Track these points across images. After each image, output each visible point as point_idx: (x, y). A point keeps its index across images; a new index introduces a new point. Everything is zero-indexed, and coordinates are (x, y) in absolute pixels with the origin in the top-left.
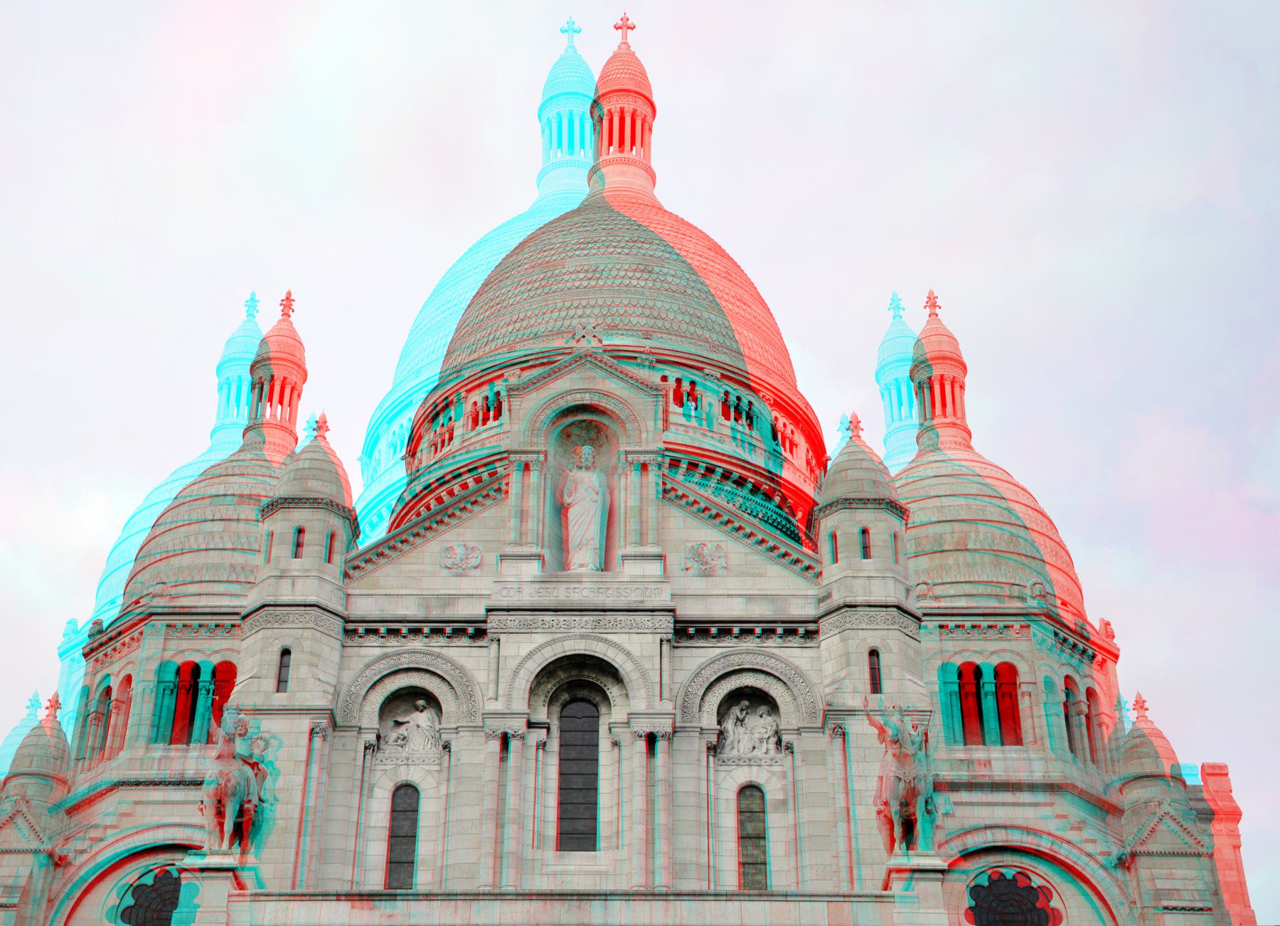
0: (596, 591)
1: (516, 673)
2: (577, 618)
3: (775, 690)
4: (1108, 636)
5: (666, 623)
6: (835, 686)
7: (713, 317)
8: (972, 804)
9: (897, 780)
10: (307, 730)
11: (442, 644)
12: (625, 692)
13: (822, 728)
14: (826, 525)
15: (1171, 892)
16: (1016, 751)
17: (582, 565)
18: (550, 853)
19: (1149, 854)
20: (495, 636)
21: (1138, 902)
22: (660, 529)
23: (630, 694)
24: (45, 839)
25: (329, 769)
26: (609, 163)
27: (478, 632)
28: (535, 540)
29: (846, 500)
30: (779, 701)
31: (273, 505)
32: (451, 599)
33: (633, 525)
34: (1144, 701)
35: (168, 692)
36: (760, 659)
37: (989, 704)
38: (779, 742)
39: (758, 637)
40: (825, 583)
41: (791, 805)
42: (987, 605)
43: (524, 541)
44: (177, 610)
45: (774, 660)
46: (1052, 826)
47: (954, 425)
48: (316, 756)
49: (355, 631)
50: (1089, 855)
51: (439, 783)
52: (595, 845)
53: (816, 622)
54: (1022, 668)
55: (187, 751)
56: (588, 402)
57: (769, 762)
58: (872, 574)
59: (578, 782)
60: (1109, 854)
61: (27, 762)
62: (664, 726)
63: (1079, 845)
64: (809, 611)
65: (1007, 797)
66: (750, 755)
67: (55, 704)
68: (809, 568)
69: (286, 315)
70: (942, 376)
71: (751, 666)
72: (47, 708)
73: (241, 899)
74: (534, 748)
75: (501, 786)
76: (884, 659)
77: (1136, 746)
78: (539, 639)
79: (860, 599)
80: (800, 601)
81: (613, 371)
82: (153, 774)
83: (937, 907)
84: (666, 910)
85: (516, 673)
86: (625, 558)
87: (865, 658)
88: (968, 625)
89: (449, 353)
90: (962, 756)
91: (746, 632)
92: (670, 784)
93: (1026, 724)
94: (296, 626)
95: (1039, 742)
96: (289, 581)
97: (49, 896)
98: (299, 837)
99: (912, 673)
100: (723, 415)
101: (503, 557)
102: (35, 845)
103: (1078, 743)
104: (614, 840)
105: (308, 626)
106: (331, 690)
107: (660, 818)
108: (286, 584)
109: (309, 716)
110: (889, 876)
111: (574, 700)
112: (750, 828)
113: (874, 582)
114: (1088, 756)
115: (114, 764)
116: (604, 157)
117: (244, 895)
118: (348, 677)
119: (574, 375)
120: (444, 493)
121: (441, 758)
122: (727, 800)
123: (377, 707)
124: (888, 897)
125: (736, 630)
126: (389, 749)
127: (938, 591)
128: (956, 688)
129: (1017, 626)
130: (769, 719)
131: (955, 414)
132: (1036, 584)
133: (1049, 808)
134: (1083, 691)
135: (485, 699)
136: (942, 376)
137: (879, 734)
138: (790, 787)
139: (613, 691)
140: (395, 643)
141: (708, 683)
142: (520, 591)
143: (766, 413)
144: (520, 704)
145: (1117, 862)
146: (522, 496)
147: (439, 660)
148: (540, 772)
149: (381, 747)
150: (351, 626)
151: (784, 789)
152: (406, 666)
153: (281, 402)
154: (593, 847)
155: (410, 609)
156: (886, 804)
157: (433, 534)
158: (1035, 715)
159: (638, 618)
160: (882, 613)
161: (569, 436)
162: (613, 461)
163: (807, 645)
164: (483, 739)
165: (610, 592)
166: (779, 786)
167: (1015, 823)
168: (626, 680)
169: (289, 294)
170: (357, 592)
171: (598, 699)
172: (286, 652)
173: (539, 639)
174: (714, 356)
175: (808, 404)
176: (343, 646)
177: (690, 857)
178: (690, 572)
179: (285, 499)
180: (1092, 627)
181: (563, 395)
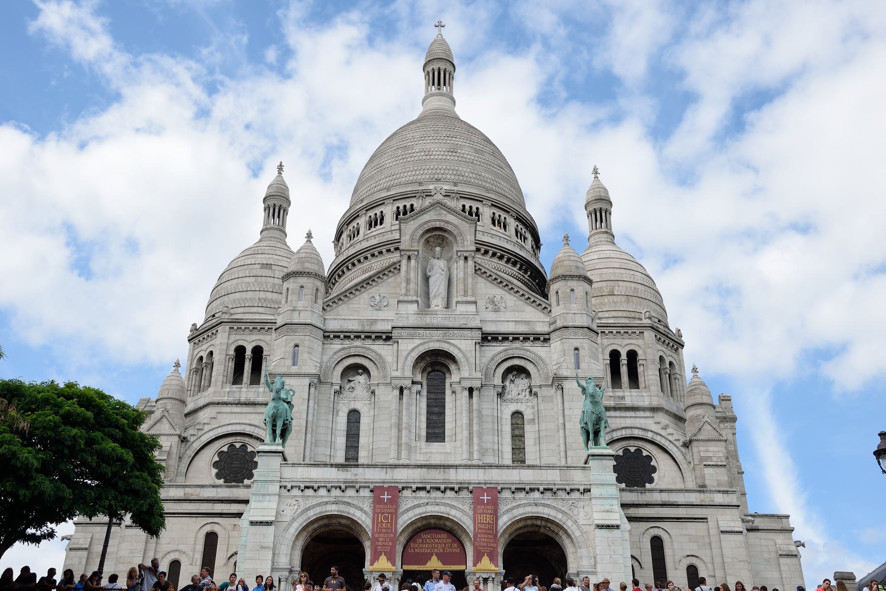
1: (406, 358)
2: (435, 332)
4: (679, 336)
5: (478, 335)
6: (558, 366)
7: (487, 175)
8: (616, 417)
10: (308, 385)
11: (370, 343)
12: (458, 367)
13: (552, 385)
14: (553, 288)
15: (709, 458)
16: (636, 392)
17: (436, 306)
18: (423, 443)
19: (698, 440)
21: (692, 463)
22: (474, 289)
23: (461, 369)
24: (177, 429)
25: (318, 402)
26: (433, 95)
31: (288, 275)
32: (374, 321)
33: (461, 286)
34: (697, 368)
35: (231, 360)
37: (624, 370)
38: (531, 391)
40: (553, 316)
41: (536, 421)
42: (623, 322)
43: (408, 293)
44: (234, 320)
47: (607, 232)
48: (312, 397)
49: (329, 336)
50: (670, 441)
51: (370, 410)
52: (444, 440)
53: (549, 334)
54: (640, 352)
55: (241, 388)
56: (439, 226)
57: (526, 401)
59: (436, 410)
60: (678, 440)
61: (166, 392)
62: (476, 384)
65: (632, 414)
66: (517, 398)
67: (177, 365)
69: (280, 173)
70: (601, 208)
71: (518, 355)
72: (174, 367)
73: (286, 465)
75: (400, 411)
76: (581, 352)
77: (693, 390)
78: (417, 342)
79: (570, 324)
80: (542, 324)
82: (226, 399)
84: (485, 473)
85: (406, 358)
86: (457, 302)
87: (572, 352)
88: (614, 332)
89: (356, 190)
90: (611, 394)
91: (515, 339)
92: (479, 412)
93: (641, 379)
94: (301, 334)
95: (647, 387)
96: (297, 312)
97: (179, 456)
98: (306, 434)
99: (594, 360)
100: (492, 224)
101: (399, 302)
102: (172, 432)
103: (665, 388)
104: (454, 438)
105: (307, 334)
106: (318, 365)
107: (475, 427)
108: (296, 314)
110: (588, 458)
111: (433, 371)
112: (517, 432)
113: (576, 315)
114: (670, 394)
115: (206, 393)
117: (287, 464)
119: (432, 213)
120: (356, 261)
121: (370, 398)
125: (511, 338)
126: (346, 393)
127: (600, 315)
129: (638, 332)
131: (607, 227)
134: (668, 363)
135: (392, 370)
136: (601, 208)
137: (583, 391)
138: (536, 413)
139: (452, 367)
143: (512, 224)
144: (408, 373)
145: (683, 444)
146: (408, 272)
147: (369, 351)
148: (417, 405)
149: (342, 392)
150: (327, 334)
153: (279, 217)
154: (443, 440)
155: (355, 326)
156: (586, 423)
158: (645, 375)
159: (464, 332)
160: (581, 331)
161: (428, 242)
162: (450, 255)
163: (545, 345)
164: (391, 389)
165: (451, 319)
168: (459, 362)
169: (281, 163)
170: (328, 317)
173: (417, 342)
174: (488, 195)
175: (532, 218)
176: (323, 344)
177: (489, 445)
179: (294, 272)
180: (672, 332)
181: (426, 223)
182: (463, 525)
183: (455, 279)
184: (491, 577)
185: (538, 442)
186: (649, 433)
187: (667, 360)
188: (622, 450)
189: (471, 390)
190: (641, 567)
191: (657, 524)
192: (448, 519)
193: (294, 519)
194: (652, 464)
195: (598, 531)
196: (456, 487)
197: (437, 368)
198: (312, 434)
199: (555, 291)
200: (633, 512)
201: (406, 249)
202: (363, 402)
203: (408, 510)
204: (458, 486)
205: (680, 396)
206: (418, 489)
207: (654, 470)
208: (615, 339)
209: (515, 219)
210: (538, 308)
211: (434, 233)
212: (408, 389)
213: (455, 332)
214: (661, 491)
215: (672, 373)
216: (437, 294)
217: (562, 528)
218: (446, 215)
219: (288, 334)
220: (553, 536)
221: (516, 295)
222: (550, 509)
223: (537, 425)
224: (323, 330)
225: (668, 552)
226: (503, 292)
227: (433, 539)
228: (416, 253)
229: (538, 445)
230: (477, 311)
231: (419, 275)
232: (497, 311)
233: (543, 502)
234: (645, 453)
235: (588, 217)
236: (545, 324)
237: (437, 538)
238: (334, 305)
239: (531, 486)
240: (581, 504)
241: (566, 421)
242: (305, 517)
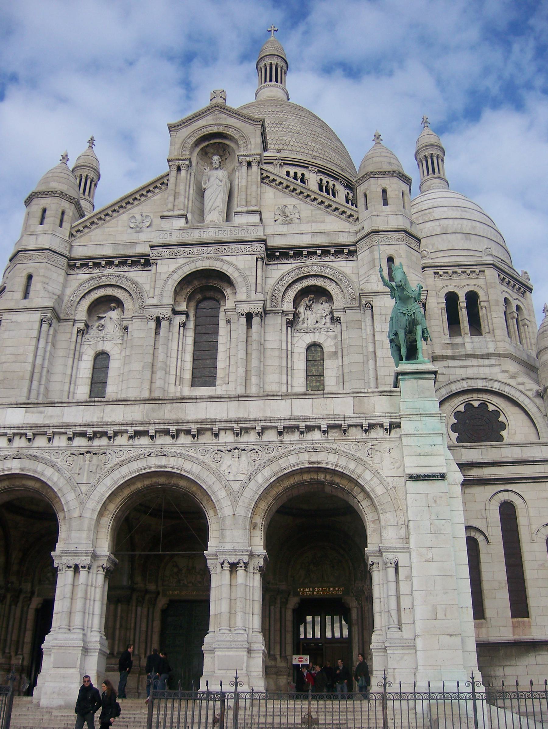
0: (217, 232)
1: (166, 281)
2: (205, 248)
3: (330, 287)
5: (260, 248)
13: (359, 306)
20: (154, 261)
28: (182, 208)
29: (371, 173)
30: (332, 293)
32: (133, 244)
36: (320, 269)
37: (463, 315)
38: (332, 318)
39: (319, 256)
45: (329, 269)
46: (501, 377)
47: (439, 178)
48: (43, 335)
50: (521, 391)
51: (121, 351)
53: (355, 244)
54: (481, 293)
56: (217, 131)
57: (326, 330)
58: (388, 213)
60: (531, 390)
63: (516, 387)
64: (351, 239)
65: (475, 362)
66: (314, 326)
68: (351, 216)
70: (432, 154)
71: (314, 273)
74: (178, 327)
78: (181, 261)
79: (381, 228)
80: (346, 235)
81: (231, 114)
83: (432, 397)
85: (166, 281)
88: (450, 272)
90: (448, 342)
91: (312, 254)
95: (491, 332)
96: (35, 237)
103: (512, 334)
104: (227, 379)
107: (254, 363)
111: (205, 299)
112: (314, 370)
113: (390, 217)
116: (263, 85)
119: (209, 118)
121: (123, 336)
122: (299, 353)
123: (86, 308)
124: (396, 392)
125: (305, 253)
126: (93, 332)
128: (444, 305)
130: (326, 306)
132: (487, 248)
133: (498, 367)
138: (340, 343)
139: (228, 292)
140: (98, 271)
141: (287, 284)
144: (168, 299)
147: (123, 279)
148: (181, 340)
150: (72, 263)
151: (336, 345)
155: (108, 251)
157: (124, 210)
159: (242, 247)
160: (396, 235)
161: (206, 154)
163: (350, 259)
165: (226, 232)
166: (333, 343)
167: (479, 377)
171: (219, 297)
176: (67, 274)
179: (36, 193)
181: (200, 129)
182: (201, 485)
185: (341, 381)
186: (496, 383)
187: (514, 303)
188: (463, 406)
189: (249, 317)
190: (488, 542)
191: (508, 487)
194: (500, 419)
195: (411, 485)
196: (194, 428)
198: (40, 381)
200: (475, 473)
201: (174, 158)
202: (114, 342)
203: (120, 465)
204: (196, 427)
205: (531, 344)
206: (138, 434)
207: (503, 426)
208: (451, 279)
209: (345, 187)
213: (231, 247)
214: (511, 445)
215: (520, 319)
216: (213, 208)
217: (357, 484)
218: (225, 119)
219: (21, 262)
220: (345, 497)
221: (313, 203)
223: (340, 358)
224: (67, 257)
225: (522, 521)
226: (298, 202)
228: (187, 162)
229: (341, 384)
230: (261, 221)
231: (191, 188)
232: (289, 223)
233: (326, 445)
234: (491, 408)
235: (419, 166)
236: (351, 234)
239: (309, 423)
240: (386, 446)
241: (377, 347)
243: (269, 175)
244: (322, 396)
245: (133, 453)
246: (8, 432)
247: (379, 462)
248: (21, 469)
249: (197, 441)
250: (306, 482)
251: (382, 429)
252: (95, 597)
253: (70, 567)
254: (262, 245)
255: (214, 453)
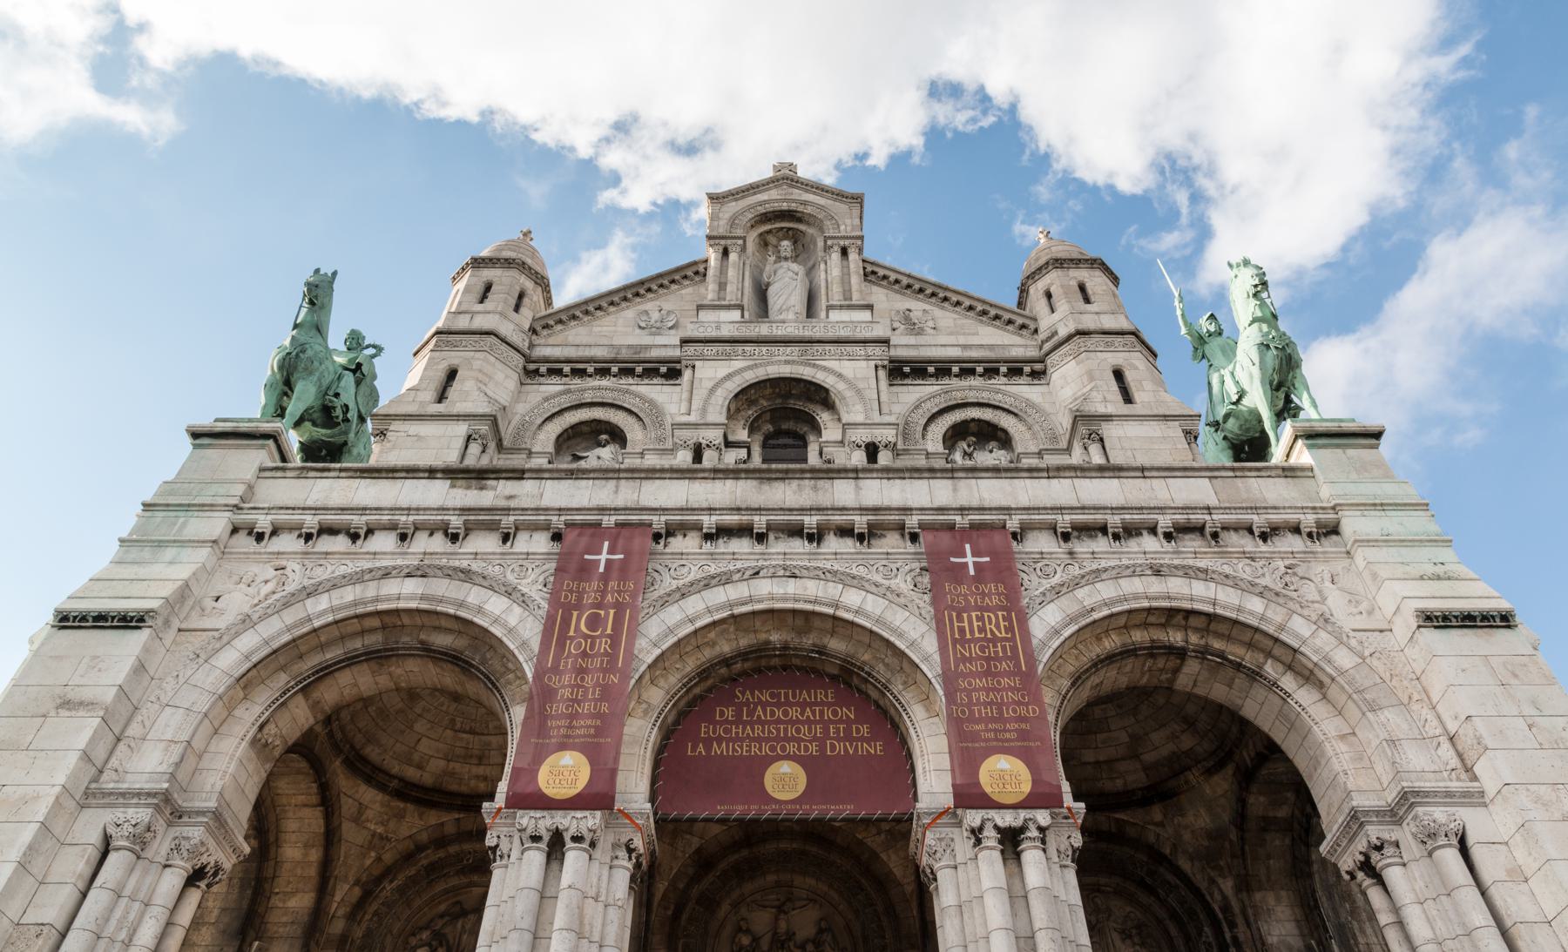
1: (712, 391)
3: (1006, 422)
9: (1265, 348)
12: (836, 417)
27: (673, 373)
29: (1057, 260)
30: (1011, 431)
49: (536, 372)
53: (1042, 361)
62: (888, 435)
64: (1032, 353)
68: (1023, 327)
73: (279, 474)
76: (1129, 376)
78: (738, 364)
86: (830, 308)
109: (468, 422)
111: (778, 433)
118: (521, 408)
123: (553, 437)
125: (955, 369)
139: (824, 417)
140: (579, 381)
142: (718, 328)
144: (717, 414)
150: (532, 367)
152: (589, 400)
159: (847, 348)
160: (1118, 340)
161: (766, 244)
172: (452, 375)
176: (522, 384)
178: (896, 332)
182: (892, 639)
183: (823, 284)
184: (1032, 826)
192: (837, 624)
193: (247, 622)
197: (785, 426)
199: (1042, 292)
203: (682, 593)
204: (865, 519)
206: (724, 532)
210: (1008, 327)
211: (778, 225)
212: (714, 448)
213: (827, 348)
218: (800, 195)
222: (1213, 585)
226: (927, 307)
227: (778, 705)
228: (740, 242)
237: (797, 704)
238: (559, 327)
242: (290, 616)
243: (876, 269)
244: (1140, 474)
245: (713, 569)
246: (404, 518)
247: (1317, 598)
248: (423, 598)
249: (869, 548)
250: (1140, 649)
251: (1297, 537)
252: (602, 937)
253: (536, 838)
254: (883, 348)
255: (913, 574)
